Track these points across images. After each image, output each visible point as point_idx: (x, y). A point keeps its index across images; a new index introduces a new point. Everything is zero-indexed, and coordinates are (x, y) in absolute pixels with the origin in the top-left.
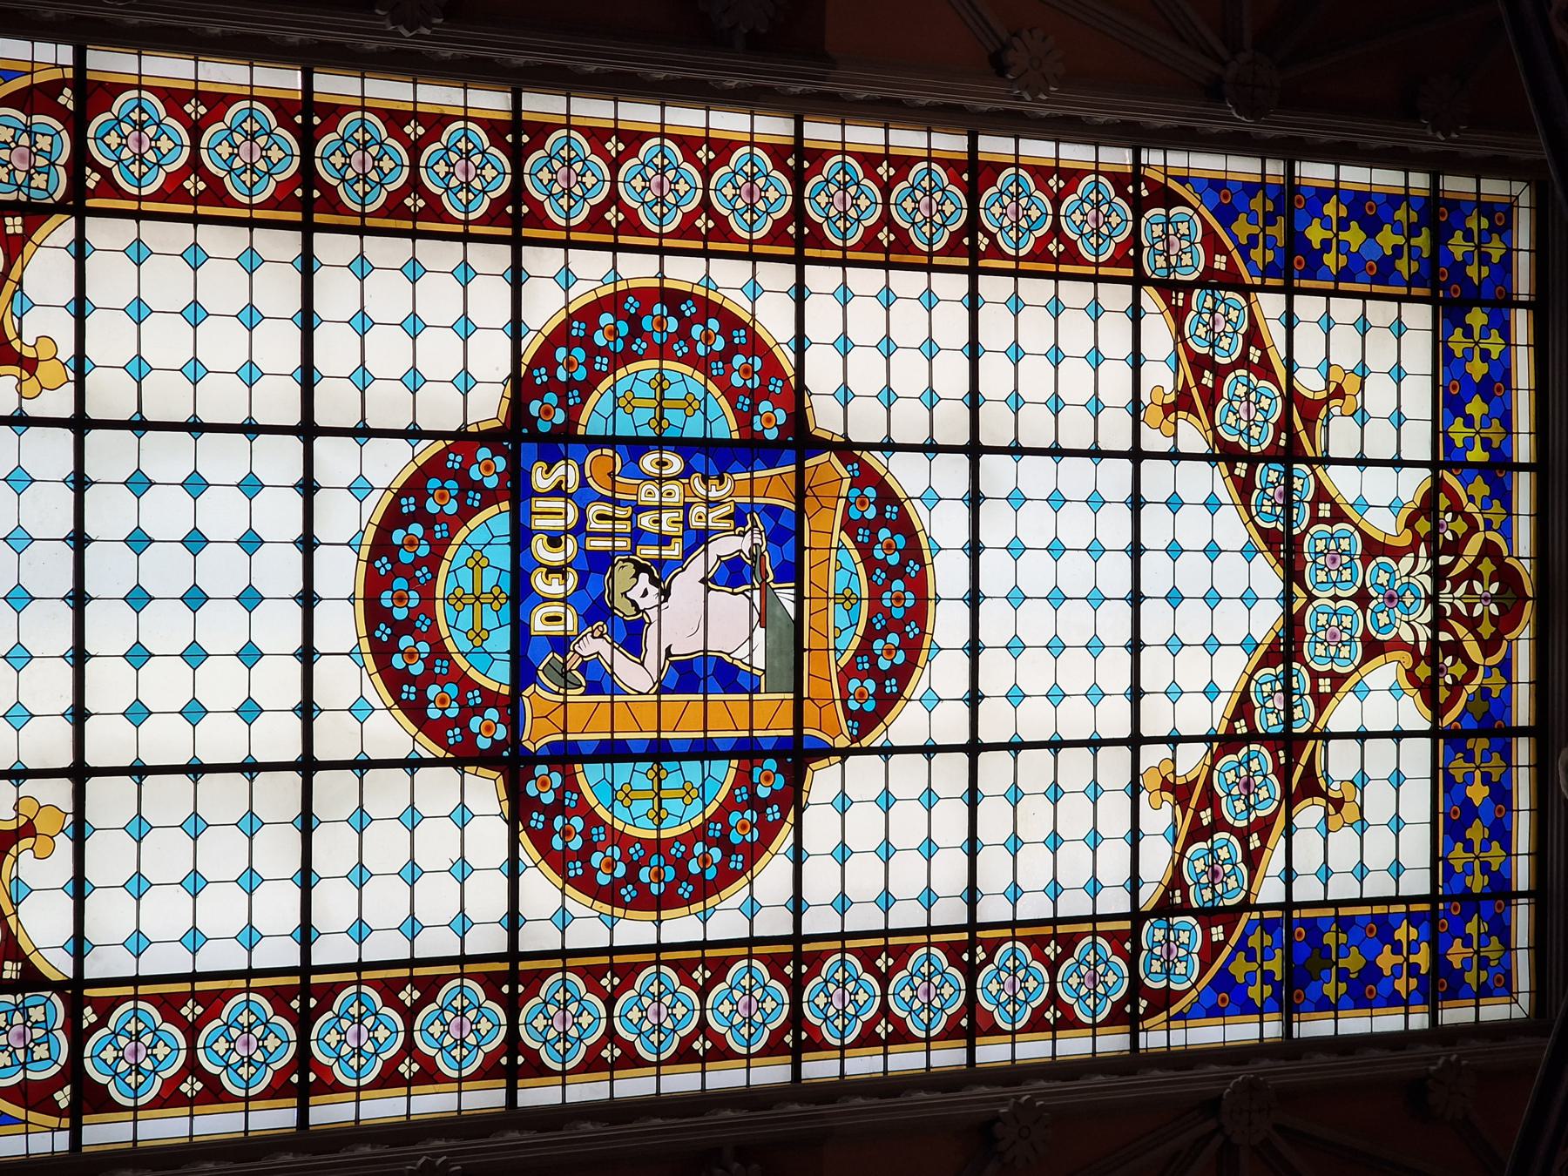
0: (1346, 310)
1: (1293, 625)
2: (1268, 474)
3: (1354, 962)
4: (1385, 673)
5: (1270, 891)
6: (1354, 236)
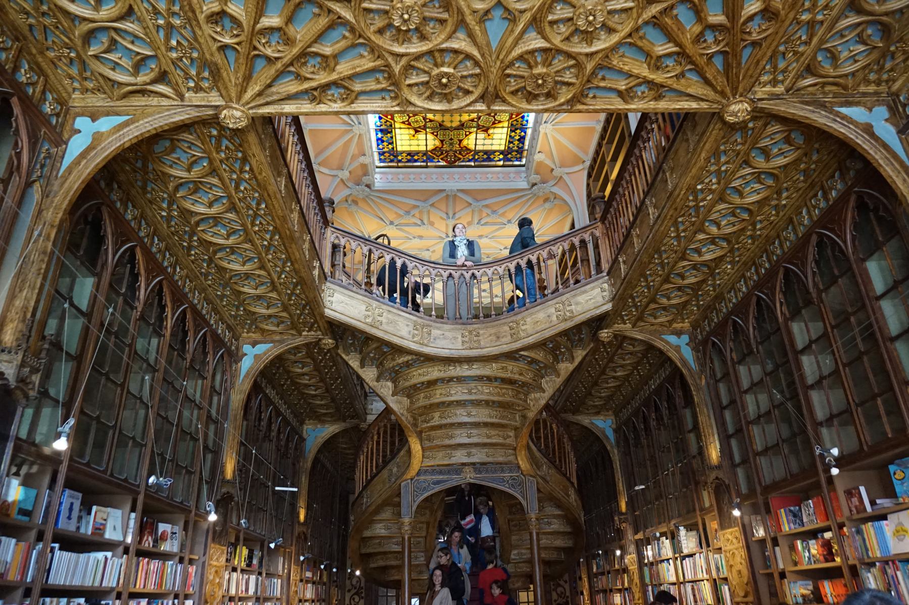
0: (504, 136)
1: (447, 129)
2: (475, 124)
3: (385, 139)
4: (438, 143)
5: (397, 125)
6: (517, 137)
